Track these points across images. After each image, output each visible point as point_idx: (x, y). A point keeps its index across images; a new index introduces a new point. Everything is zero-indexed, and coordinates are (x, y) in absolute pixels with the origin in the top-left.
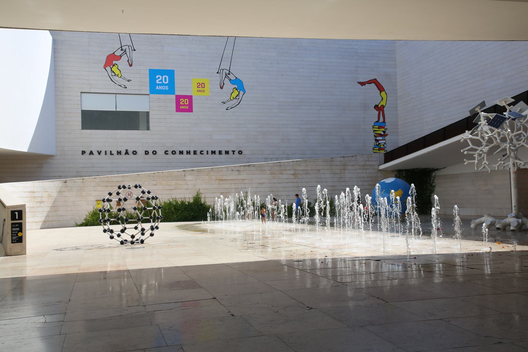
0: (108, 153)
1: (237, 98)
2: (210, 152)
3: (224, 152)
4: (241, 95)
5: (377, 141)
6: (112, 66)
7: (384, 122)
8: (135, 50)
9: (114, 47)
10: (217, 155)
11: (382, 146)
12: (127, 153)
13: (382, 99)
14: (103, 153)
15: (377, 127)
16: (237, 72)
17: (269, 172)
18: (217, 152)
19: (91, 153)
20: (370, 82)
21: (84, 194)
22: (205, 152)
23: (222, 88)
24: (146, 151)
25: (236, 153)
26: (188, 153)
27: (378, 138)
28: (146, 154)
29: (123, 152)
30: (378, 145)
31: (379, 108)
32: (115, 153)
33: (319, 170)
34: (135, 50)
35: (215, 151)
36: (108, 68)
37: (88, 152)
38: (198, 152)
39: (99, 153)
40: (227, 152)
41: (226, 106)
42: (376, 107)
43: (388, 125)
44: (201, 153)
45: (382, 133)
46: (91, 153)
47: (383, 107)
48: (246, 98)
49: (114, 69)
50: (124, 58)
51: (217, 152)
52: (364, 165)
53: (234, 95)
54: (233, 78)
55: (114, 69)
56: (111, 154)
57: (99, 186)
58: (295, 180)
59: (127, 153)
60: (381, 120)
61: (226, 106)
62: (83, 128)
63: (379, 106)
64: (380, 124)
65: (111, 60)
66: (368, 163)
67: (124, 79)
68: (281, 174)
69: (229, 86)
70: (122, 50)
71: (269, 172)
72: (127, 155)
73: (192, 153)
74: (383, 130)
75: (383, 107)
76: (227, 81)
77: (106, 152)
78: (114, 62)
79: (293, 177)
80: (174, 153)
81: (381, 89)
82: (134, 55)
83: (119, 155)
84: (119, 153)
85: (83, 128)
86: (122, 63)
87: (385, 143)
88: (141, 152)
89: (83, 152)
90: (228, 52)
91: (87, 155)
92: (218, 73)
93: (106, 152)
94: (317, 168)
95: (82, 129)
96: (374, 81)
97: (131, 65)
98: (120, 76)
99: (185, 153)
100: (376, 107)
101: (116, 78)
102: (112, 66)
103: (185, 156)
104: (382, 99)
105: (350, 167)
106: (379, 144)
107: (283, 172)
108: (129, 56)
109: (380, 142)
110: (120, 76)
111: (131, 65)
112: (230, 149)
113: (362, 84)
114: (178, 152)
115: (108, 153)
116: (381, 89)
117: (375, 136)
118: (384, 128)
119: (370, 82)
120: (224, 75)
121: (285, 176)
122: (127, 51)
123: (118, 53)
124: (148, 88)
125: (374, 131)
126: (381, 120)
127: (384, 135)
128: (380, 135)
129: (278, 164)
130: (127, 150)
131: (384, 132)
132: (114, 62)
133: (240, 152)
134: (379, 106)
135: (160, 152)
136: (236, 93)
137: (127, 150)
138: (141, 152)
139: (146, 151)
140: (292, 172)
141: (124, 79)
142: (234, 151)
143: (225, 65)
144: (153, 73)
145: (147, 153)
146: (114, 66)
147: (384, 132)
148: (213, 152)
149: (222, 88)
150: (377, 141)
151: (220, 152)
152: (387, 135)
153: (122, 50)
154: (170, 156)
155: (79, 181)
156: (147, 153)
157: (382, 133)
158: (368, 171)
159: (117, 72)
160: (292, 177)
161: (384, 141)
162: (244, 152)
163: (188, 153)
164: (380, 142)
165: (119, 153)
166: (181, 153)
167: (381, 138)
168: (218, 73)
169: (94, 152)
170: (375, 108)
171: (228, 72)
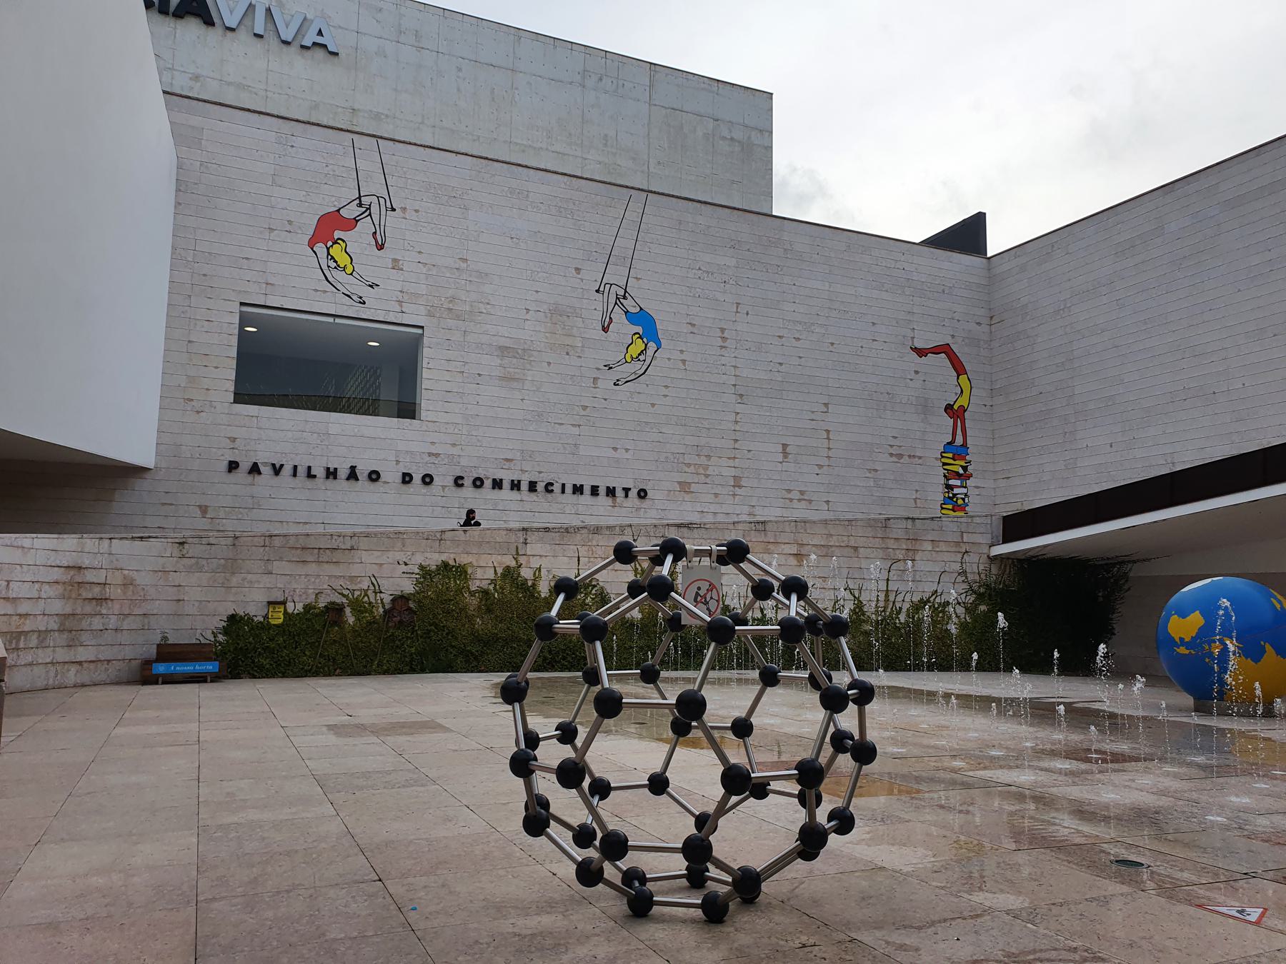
0: (302, 471)
1: (642, 358)
2: (569, 489)
3: (602, 491)
4: (650, 352)
6: (330, 243)
7: (964, 445)
8: (393, 210)
9: (339, 196)
10: (586, 497)
12: (353, 475)
14: (287, 470)
15: (950, 455)
16: (644, 296)
18: (587, 490)
20: (936, 350)
21: (235, 580)
22: (557, 488)
23: (605, 329)
24: (404, 475)
25: (633, 494)
27: (951, 482)
28: (404, 482)
29: (343, 473)
31: (955, 413)
32: (319, 471)
33: (856, 548)
34: (393, 210)
35: (582, 486)
36: (320, 248)
37: (245, 465)
38: (540, 487)
39: (277, 470)
40: (611, 492)
41: (613, 375)
42: (949, 408)
44: (548, 488)
45: (961, 471)
46: (255, 469)
47: (963, 409)
50: (365, 226)
51: (587, 490)
52: (957, 544)
53: (634, 351)
56: (310, 476)
57: (281, 559)
61: (613, 375)
62: (241, 397)
63: (956, 407)
64: (955, 450)
65: (329, 228)
67: (361, 278)
69: (623, 328)
70: (360, 205)
72: (352, 482)
73: (524, 486)
74: (963, 463)
75: (963, 409)
76: (618, 315)
77: (295, 467)
78: (337, 234)
79: (795, 562)
80: (478, 483)
81: (959, 369)
82: (391, 220)
83: (330, 482)
84: (331, 474)
85: (241, 397)
88: (391, 475)
89: (233, 466)
90: (625, 243)
91: (241, 475)
92: (597, 291)
93: (295, 467)
94: (852, 543)
95: (240, 398)
98: (349, 270)
99: (506, 485)
100: (949, 408)
101: (339, 275)
102: (330, 243)
103: (506, 493)
106: (955, 495)
107: (770, 546)
108: (377, 223)
110: (349, 270)
111: (380, 247)
112: (619, 485)
113: (921, 352)
114: (488, 483)
115: (302, 471)
116: (959, 369)
118: (964, 458)
119: (936, 350)
120: (613, 299)
122: (375, 209)
123: (350, 212)
125: (944, 464)
126: (959, 440)
127: (965, 476)
128: (958, 476)
129: (760, 527)
130: (353, 468)
131: (965, 468)
132: (337, 234)
133: (642, 494)
134: (956, 407)
135: (443, 479)
137: (353, 468)
138: (391, 475)
139: (404, 475)
141: (361, 278)
142: (627, 490)
143: (616, 275)
145: (407, 478)
146: (335, 242)
147: (965, 468)
148: (578, 489)
149: (605, 329)
153: (360, 205)
155: (223, 541)
156: (407, 478)
157: (961, 471)
159: (343, 260)
160: (793, 561)
161: (964, 491)
164: (956, 491)
166: (497, 484)
167: (958, 483)
168: (597, 291)
169: (262, 468)
171: (621, 292)
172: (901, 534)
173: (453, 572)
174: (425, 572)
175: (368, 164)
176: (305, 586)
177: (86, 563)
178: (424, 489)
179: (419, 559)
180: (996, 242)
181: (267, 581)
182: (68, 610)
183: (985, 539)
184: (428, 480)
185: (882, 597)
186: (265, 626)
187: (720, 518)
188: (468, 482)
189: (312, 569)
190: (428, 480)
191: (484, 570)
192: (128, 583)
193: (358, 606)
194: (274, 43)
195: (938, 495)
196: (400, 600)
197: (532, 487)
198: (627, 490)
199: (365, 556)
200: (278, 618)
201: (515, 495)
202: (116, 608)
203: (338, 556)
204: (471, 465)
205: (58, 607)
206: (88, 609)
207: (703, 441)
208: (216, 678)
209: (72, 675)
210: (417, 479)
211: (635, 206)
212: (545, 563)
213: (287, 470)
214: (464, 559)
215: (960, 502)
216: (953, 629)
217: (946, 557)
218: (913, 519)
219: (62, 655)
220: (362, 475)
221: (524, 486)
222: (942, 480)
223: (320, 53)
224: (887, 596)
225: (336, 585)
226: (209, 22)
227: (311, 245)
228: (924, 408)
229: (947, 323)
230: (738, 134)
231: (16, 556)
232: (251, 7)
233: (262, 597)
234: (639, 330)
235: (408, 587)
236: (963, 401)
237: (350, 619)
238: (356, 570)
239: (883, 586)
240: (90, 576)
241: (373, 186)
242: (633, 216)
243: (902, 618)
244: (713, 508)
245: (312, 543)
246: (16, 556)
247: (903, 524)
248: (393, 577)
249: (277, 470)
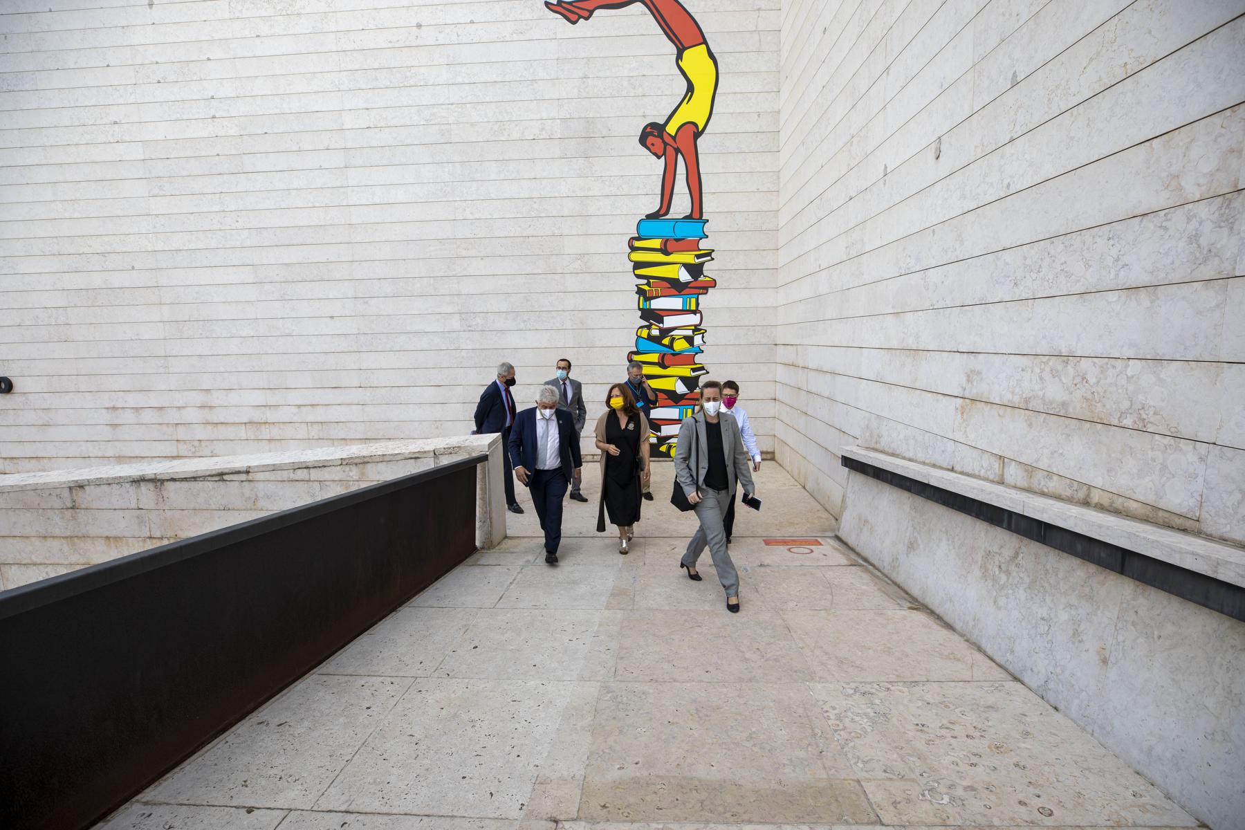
5: (651, 316)
7: (696, 215)
11: (680, 345)
13: (691, 88)
15: (656, 243)
27: (656, 304)
30: (657, 340)
31: (670, 143)
42: (653, 135)
43: (719, 234)
45: (684, 276)
47: (694, 132)
60: (681, 204)
63: (671, 129)
74: (690, 258)
75: (694, 132)
87: (696, 329)
100: (653, 135)
104: (691, 88)
106: (665, 332)
109: (669, 322)
117: (640, 292)
118: (694, 246)
125: (638, 265)
126: (681, 204)
127: (696, 283)
128: (676, 287)
131: (695, 270)
134: (671, 129)
147: (695, 270)
150: (651, 316)
152: (714, 283)
157: (684, 276)
161: (693, 319)
164: (669, 322)
167: (676, 303)
170: (643, 140)
187: (148, 416)
207: (97, 280)
215: (680, 345)
218: (157, 482)
222: (632, 301)
228: (586, 139)
236: (694, 112)
244: (133, 400)
247: (130, 496)
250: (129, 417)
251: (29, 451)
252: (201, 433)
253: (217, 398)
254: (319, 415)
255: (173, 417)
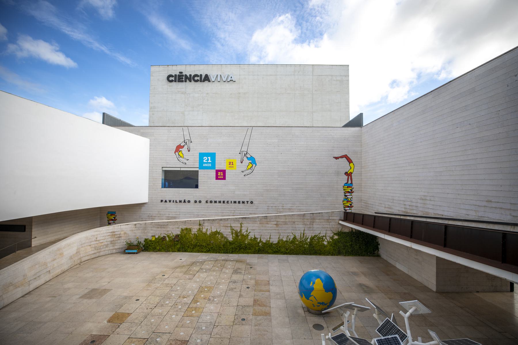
2: (233, 202)
3: (241, 202)
7: (352, 183)
9: (180, 141)
10: (237, 204)
12: (185, 202)
14: (172, 201)
16: (252, 153)
17: (259, 222)
18: (237, 202)
19: (166, 201)
20: (342, 157)
21: (146, 231)
22: (230, 202)
23: (242, 162)
25: (249, 202)
26: (220, 202)
29: (183, 201)
31: (349, 175)
32: (178, 201)
33: (294, 222)
36: (177, 153)
37: (164, 201)
38: (226, 202)
40: (243, 202)
41: (244, 174)
42: (346, 173)
44: (228, 202)
46: (166, 201)
48: (257, 169)
49: (180, 153)
50: (186, 147)
53: (249, 167)
54: (249, 156)
55: (180, 153)
56: (176, 202)
58: (277, 229)
59: (185, 202)
60: (350, 182)
61: (244, 174)
62: (164, 186)
65: (179, 148)
66: (331, 218)
68: (268, 224)
69: (246, 162)
71: (259, 222)
73: (222, 202)
75: (351, 173)
80: (211, 202)
81: (350, 161)
82: (191, 145)
84: (180, 201)
86: (184, 150)
88: (192, 201)
89: (162, 201)
90: (247, 140)
94: (293, 220)
96: (346, 157)
97: (189, 151)
99: (218, 202)
100: (346, 173)
101: (181, 159)
103: (218, 204)
105: (317, 221)
111: (189, 151)
112: (245, 200)
113: (337, 158)
114: (213, 202)
116: (350, 161)
119: (342, 157)
120: (243, 155)
121: (270, 225)
124: (198, 164)
126: (350, 182)
127: (351, 192)
128: (349, 192)
131: (351, 190)
133: (252, 202)
135: (203, 202)
136: (251, 165)
138: (192, 201)
140: (275, 223)
142: (247, 202)
143: (244, 149)
144: (202, 155)
145: (196, 202)
147: (351, 190)
148: (235, 202)
149: (242, 162)
150: (346, 196)
151: (239, 202)
154: (209, 204)
156: (196, 202)
158: (331, 224)
159: (181, 155)
160: (275, 226)
162: (254, 202)
163: (220, 202)
165: (180, 201)
166: (215, 202)
167: (349, 194)
172: (309, 218)
173: (189, 230)
174: (182, 230)
175: (186, 133)
176: (159, 233)
177: (115, 230)
178: (200, 204)
179: (181, 227)
180: (365, 123)
181: (151, 232)
182: (112, 240)
183: (338, 218)
184: (200, 202)
185: (302, 235)
186: (151, 241)
188: (209, 202)
189: (160, 229)
190: (200, 202)
191: (195, 230)
192: (125, 233)
193: (168, 236)
194: (222, 82)
195: (342, 197)
196: (177, 236)
197: (224, 202)
198: (247, 202)
199: (170, 227)
200: (154, 239)
201: (220, 204)
202: (123, 238)
203: (164, 226)
204: (209, 198)
205: (110, 239)
206: (117, 239)
207: (268, 188)
208: (137, 253)
209: (114, 251)
210: (198, 202)
211: (249, 131)
212: (209, 228)
213: (172, 201)
214: (190, 227)
216: (325, 243)
217: (324, 223)
219: (111, 248)
220: (187, 201)
221: (222, 202)
222: (343, 194)
223: (231, 82)
224: (304, 235)
225: (165, 232)
226: (209, 81)
227: (175, 153)
229: (346, 148)
230: (339, 78)
231: (98, 233)
232: (217, 75)
233: (151, 235)
234: (251, 161)
235: (179, 233)
236: (351, 171)
237: (167, 239)
238: (168, 229)
239: (302, 232)
240: (116, 233)
241: (187, 137)
242: (249, 133)
243: (309, 240)
244: (271, 205)
245: (160, 224)
246: (98, 233)
248: (176, 231)
249: (170, 201)
250: (271, 208)
251: (253, 212)
252: (281, 210)
253: (284, 205)
254: (299, 208)
255: (277, 208)
